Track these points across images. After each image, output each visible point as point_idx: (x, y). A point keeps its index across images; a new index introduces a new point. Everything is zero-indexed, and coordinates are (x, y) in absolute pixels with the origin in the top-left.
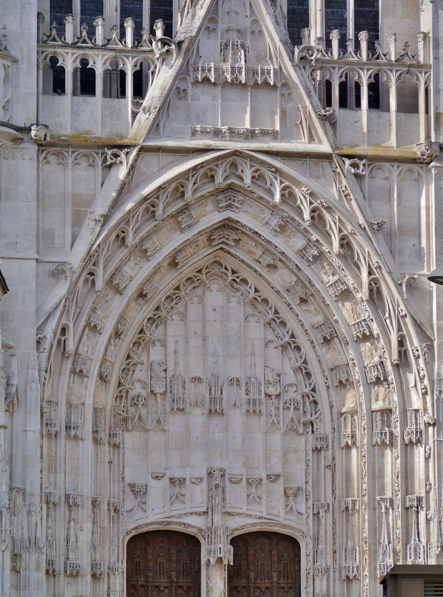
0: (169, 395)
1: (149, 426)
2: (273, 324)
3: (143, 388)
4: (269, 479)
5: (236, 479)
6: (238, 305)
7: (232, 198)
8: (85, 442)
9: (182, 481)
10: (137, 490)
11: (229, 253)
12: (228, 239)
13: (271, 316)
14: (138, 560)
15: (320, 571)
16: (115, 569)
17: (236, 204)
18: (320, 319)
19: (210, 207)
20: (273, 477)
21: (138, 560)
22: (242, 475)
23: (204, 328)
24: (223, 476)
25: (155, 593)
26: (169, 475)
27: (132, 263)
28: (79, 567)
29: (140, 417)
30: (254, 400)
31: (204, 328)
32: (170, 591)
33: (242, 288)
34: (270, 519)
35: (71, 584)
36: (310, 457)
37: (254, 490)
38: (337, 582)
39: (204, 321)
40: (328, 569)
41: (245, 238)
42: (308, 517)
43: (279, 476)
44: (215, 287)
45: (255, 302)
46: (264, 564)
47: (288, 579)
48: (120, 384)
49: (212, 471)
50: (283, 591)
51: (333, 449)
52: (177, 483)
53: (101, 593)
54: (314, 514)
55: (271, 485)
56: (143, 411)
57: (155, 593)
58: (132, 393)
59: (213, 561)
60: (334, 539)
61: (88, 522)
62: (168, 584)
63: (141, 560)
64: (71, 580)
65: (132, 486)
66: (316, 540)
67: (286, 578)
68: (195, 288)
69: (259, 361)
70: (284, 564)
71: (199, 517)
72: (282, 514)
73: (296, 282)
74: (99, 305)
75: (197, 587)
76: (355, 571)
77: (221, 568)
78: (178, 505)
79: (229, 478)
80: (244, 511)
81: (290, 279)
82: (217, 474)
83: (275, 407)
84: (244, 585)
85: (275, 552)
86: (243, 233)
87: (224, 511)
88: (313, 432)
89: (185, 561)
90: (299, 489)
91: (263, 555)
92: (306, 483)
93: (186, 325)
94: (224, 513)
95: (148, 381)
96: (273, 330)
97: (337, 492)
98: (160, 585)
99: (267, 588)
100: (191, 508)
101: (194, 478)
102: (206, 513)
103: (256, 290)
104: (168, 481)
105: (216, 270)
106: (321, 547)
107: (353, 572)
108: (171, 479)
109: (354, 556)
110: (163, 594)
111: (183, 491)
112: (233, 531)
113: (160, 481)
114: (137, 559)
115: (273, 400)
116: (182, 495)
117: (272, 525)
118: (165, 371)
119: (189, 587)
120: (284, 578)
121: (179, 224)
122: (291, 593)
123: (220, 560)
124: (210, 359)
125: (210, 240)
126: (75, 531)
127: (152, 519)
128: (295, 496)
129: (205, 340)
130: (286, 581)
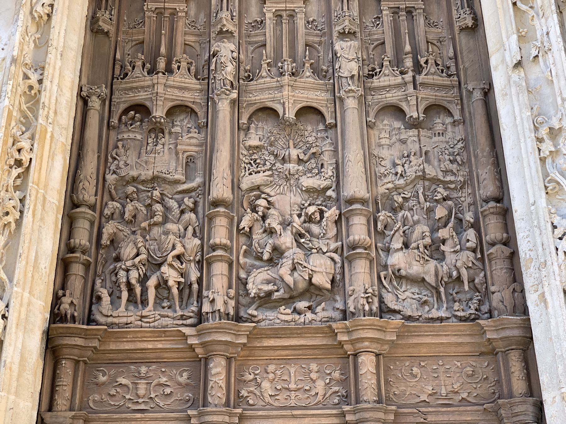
46: (292, 16)
47: (418, 68)
50: (397, 124)
67: (409, 63)
70: (395, 11)
84: (187, 97)
120: (398, 62)
130: (409, 77)
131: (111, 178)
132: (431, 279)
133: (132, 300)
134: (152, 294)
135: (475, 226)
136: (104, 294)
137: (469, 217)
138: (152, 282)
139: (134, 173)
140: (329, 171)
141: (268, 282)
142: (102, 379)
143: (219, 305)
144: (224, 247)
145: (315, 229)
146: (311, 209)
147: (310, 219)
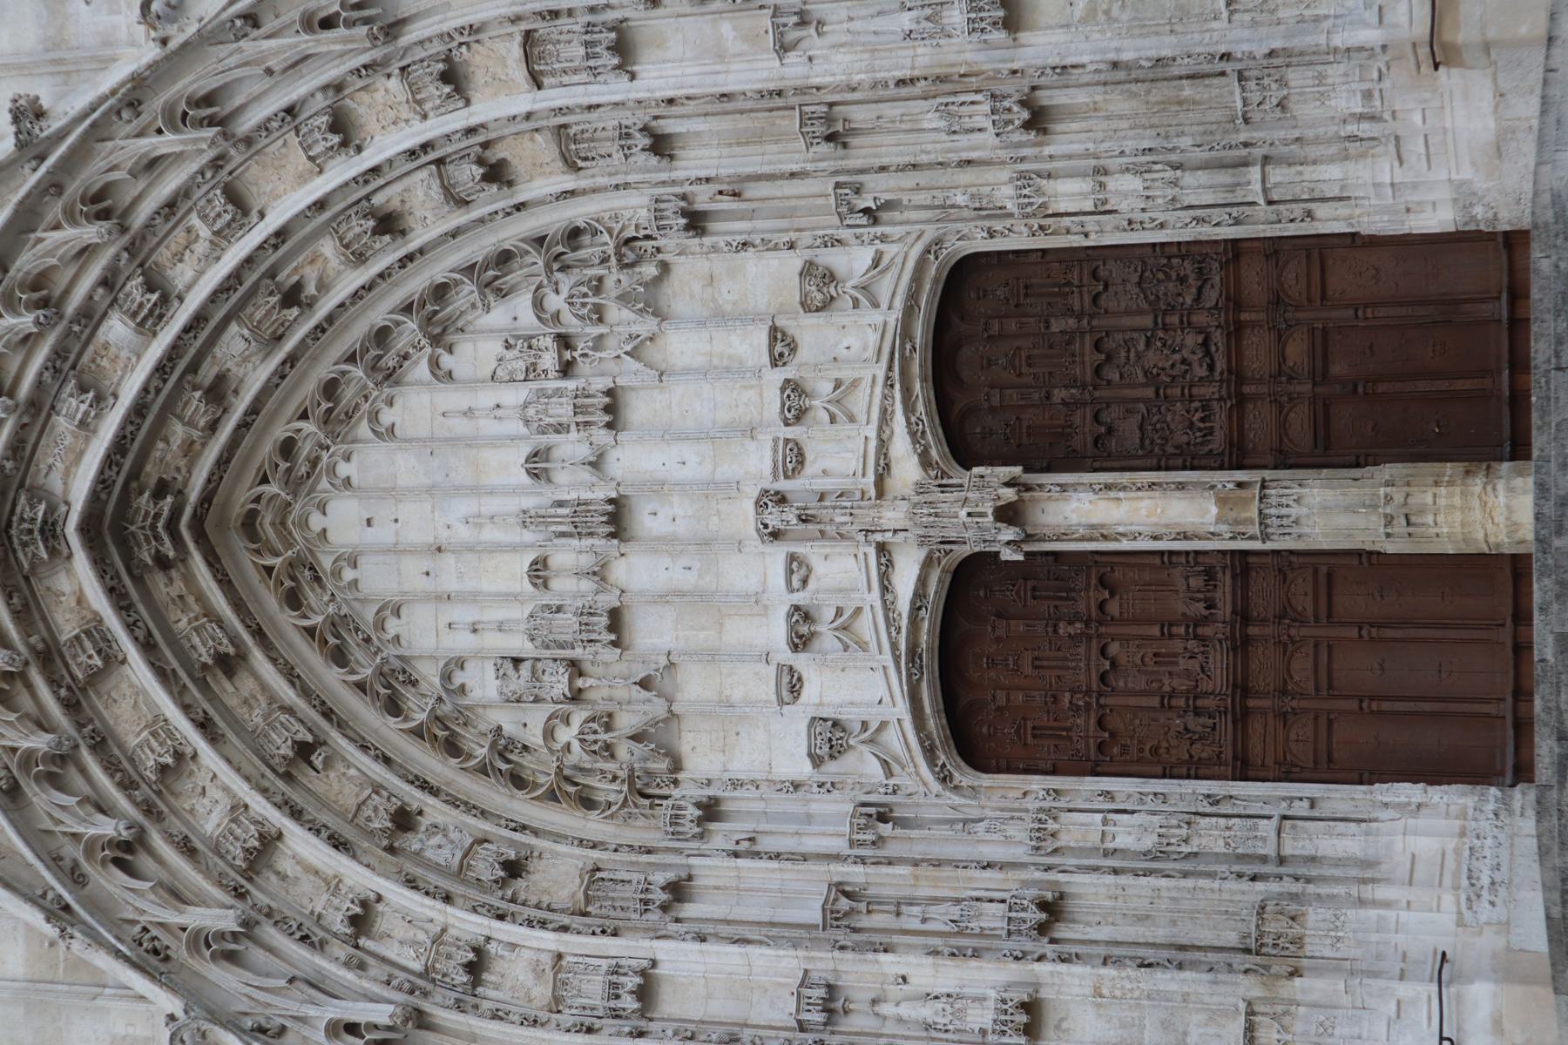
0: (578, 653)
1: (659, 709)
2: (390, 361)
3: (567, 721)
4: (785, 360)
5: (788, 459)
6: (355, 457)
7: (26, 525)
8: (659, 957)
9: (802, 614)
10: (826, 748)
11: (206, 499)
12: (157, 516)
13: (358, 372)
14: (1029, 731)
15: (1026, 200)
16: (1039, 830)
17: (40, 514)
18: (328, 248)
19: (63, 583)
20: (779, 348)
21: (1029, 731)
22: (776, 440)
23: (412, 551)
24: (782, 499)
25: (1121, 684)
26: (785, 655)
27: (201, 805)
28: (1004, 1001)
29: (637, 738)
30: (577, 409)
31: (412, 551)
32: (1113, 640)
33: (305, 449)
34: (892, 353)
35: (1062, 1020)
36: (721, 241)
37: (816, 403)
38: (1047, 151)
39: (396, 550)
40: (1022, 175)
41: (148, 468)
42: (883, 238)
43: (774, 330)
44: (316, 522)
45: (339, 414)
47: (1068, 284)
48: (552, 796)
49: (766, 531)
50: (1104, 296)
51: (681, 183)
52: (804, 629)
53: (1103, 890)
54: (876, 221)
55: (804, 354)
56: (627, 721)
57: (1121, 684)
58: (577, 754)
59: (1009, 533)
60: (930, 166)
61: (877, 962)
62: (1094, 643)
63: (1029, 725)
64: (1050, 1018)
65: (816, 761)
66: (945, 209)
67: (1067, 289)
68: (317, 579)
69: (486, 398)
71: (896, 566)
72: (877, 317)
73: (241, 322)
74: (305, 901)
75: (1098, 558)
76: (1006, 104)
77: (1033, 500)
78: (864, 626)
79: (786, 477)
80: (872, 432)
81: (234, 341)
82: (774, 519)
83: (595, 348)
85: (995, 327)
86: (136, 473)
87: (872, 492)
88: (648, 237)
89: (1029, 593)
90: (808, 269)
91: (1001, 361)
92: (792, 246)
93: (409, 602)
94: (880, 494)
95: (552, 708)
96: (406, 357)
97: (795, 168)
98: (1098, 671)
99: (1097, 346)
100: (870, 590)
101: (789, 582)
102: (882, 548)
103: (304, 416)
104: (802, 656)
105: (266, 520)
106: (960, 199)
107: (1009, 110)
108: (795, 648)
109: (964, 108)
110: (1123, 660)
111: (829, 613)
112: (925, 462)
113: (804, 678)
114: (1025, 734)
115: (576, 354)
116: (839, 612)
117: (908, 346)
118: (517, 661)
119: (1102, 582)
121: (95, 677)
122: (1111, 271)
123: (1008, 514)
124: (490, 534)
125: (163, 563)
126: (909, 999)
127: (902, 709)
128: (830, 277)
129: (439, 549)
131: (1140, 452)
132: (1199, 283)
133: (1211, 434)
134: (1208, 425)
135: (1169, 258)
136: (1207, 449)
137: (1165, 261)
138: (1202, 425)
139: (1138, 441)
140: (1135, 335)
141: (1201, 366)
142: (1251, 445)
143: (1216, 390)
144: (1183, 388)
145: (1169, 342)
146: (1159, 344)
147: (1164, 345)
